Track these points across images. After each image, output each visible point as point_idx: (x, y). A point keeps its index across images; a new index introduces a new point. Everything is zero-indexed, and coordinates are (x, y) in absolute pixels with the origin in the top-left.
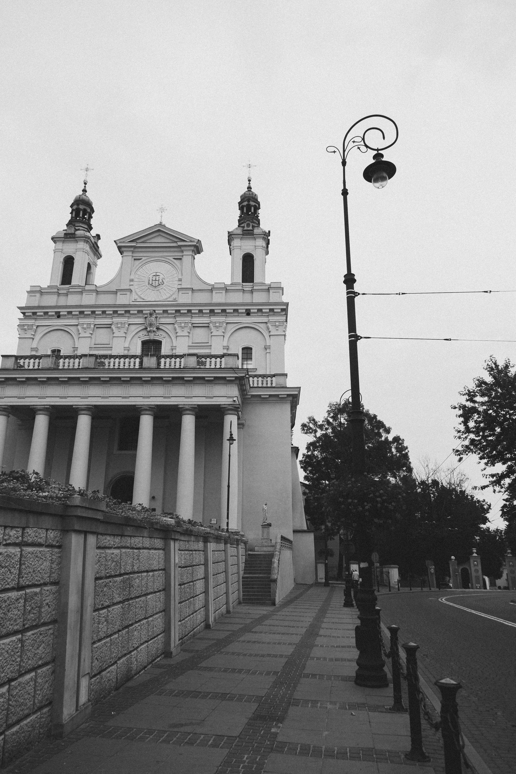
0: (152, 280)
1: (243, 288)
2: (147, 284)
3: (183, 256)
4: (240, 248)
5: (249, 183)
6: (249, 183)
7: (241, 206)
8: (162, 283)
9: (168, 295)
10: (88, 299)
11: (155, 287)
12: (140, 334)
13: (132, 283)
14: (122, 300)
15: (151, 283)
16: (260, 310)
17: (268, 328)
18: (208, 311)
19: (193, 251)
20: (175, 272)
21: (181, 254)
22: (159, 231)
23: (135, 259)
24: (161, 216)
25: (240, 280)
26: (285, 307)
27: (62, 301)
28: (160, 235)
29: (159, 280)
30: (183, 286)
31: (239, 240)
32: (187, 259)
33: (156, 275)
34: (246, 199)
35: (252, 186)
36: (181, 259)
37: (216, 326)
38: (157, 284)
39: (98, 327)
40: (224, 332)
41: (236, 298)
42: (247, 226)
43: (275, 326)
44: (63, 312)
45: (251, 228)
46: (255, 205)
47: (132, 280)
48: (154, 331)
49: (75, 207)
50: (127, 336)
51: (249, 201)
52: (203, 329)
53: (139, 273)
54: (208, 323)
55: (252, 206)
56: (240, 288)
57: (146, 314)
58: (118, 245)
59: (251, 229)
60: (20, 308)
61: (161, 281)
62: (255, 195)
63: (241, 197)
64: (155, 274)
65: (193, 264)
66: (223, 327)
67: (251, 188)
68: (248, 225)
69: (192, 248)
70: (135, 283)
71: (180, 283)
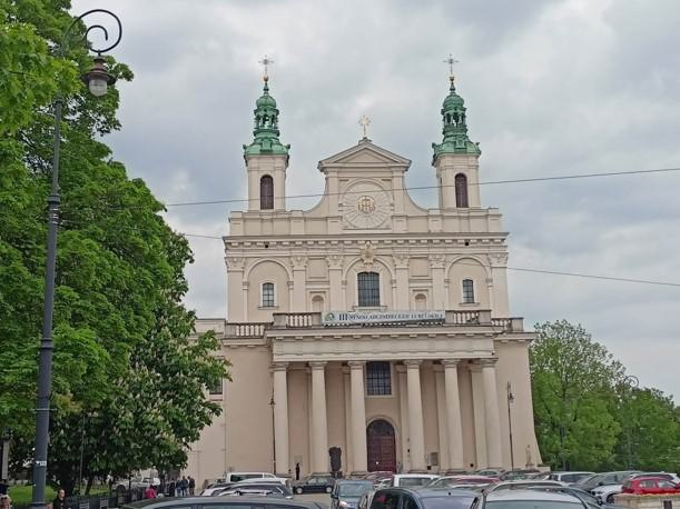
4: (452, 167)
10: (297, 229)
14: (335, 228)
17: (489, 260)
21: (390, 175)
27: (268, 229)
30: (397, 213)
32: (397, 183)
39: (311, 258)
41: (453, 226)
44: (272, 241)
47: (341, 205)
49: (262, 113)
56: (455, 214)
60: (224, 238)
70: (344, 209)
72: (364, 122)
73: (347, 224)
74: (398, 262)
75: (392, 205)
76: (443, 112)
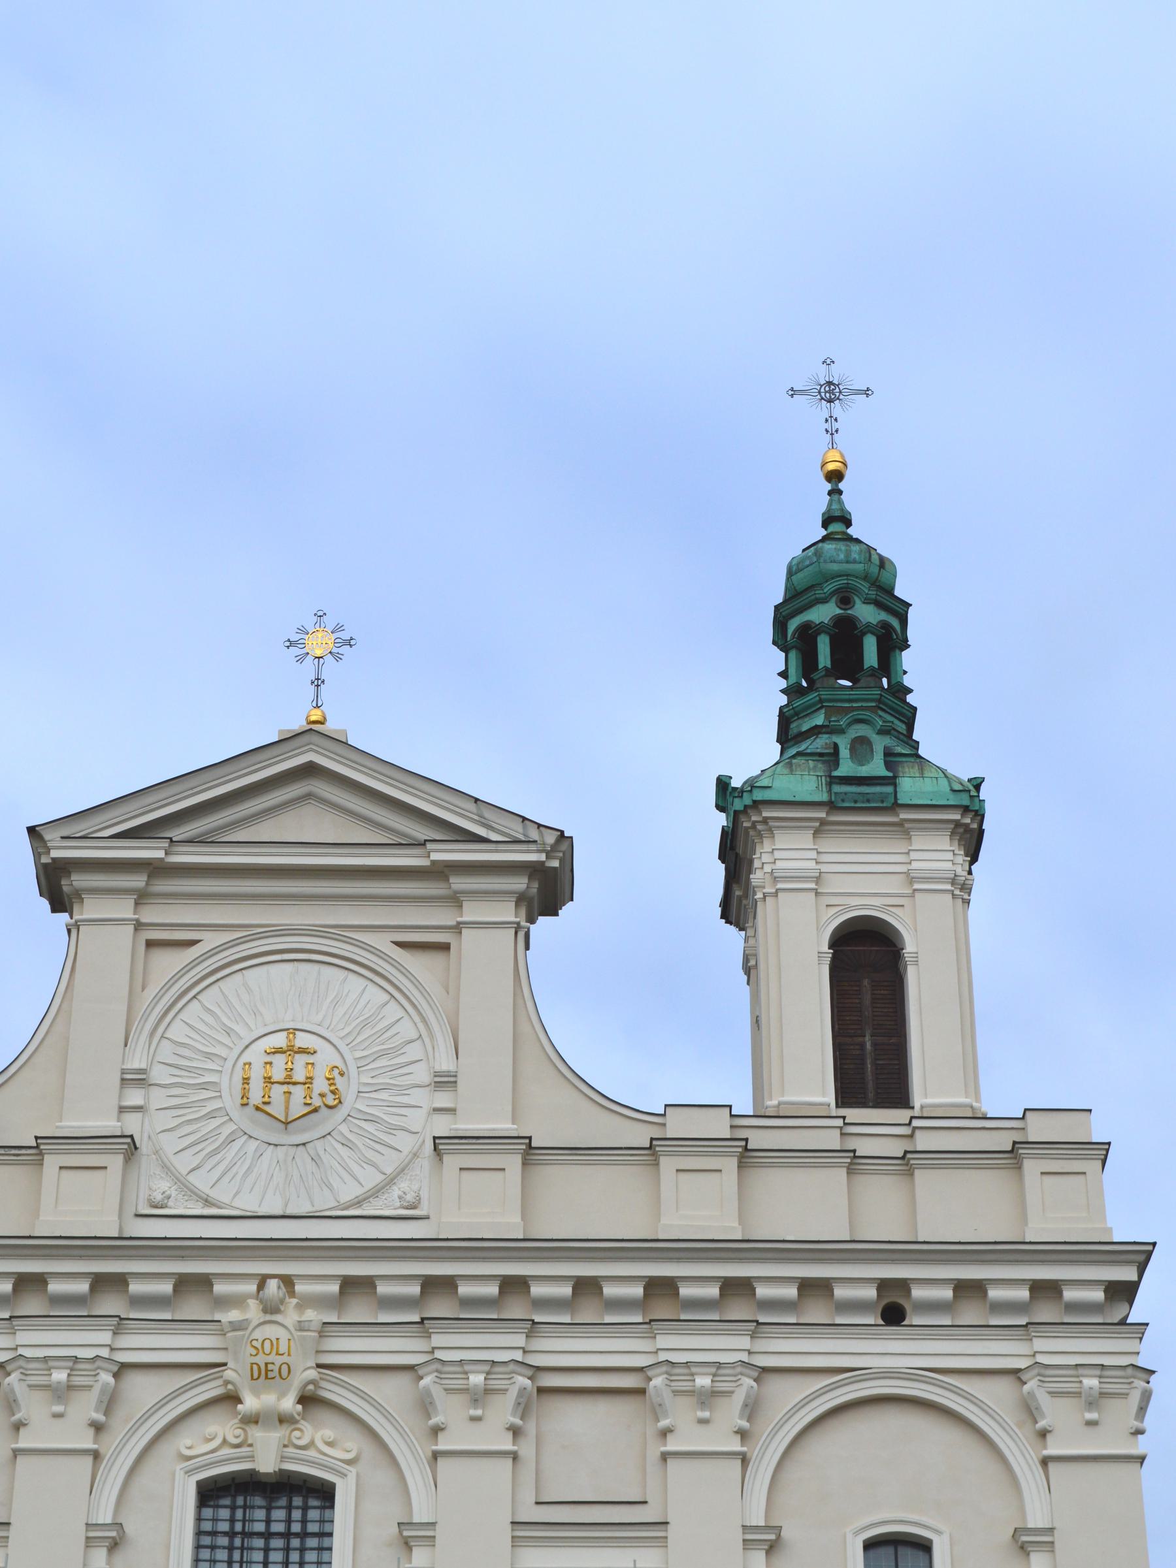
0: (268, 1080)
1: (851, 1144)
2: (230, 1101)
3: (458, 928)
5: (835, 492)
6: (835, 492)
7: (793, 625)
8: (330, 1100)
9: (371, 1179)
11: (287, 1123)
12: (189, 1441)
13: (135, 1097)
15: (256, 1097)
16: (969, 1290)
17: (1030, 1410)
18: (638, 1291)
19: (521, 899)
20: (407, 1029)
21: (445, 917)
22: (310, 770)
23: (150, 944)
24: (318, 682)
25: (831, 1098)
26: (1129, 1274)
28: (309, 796)
29: (309, 1080)
31: (805, 839)
33: (291, 1051)
34: (828, 588)
35: (850, 501)
36: (445, 947)
37: (691, 1393)
38: (297, 1110)
40: (743, 1434)
42: (853, 750)
43: (1078, 1394)
45: (876, 767)
46: (885, 626)
47: (135, 1079)
48: (284, 1420)
50: (108, 1446)
51: (845, 601)
52: (602, 1408)
53: (177, 1031)
54: (641, 1370)
55: (869, 629)
56: (832, 1140)
57: (237, 1301)
58: (54, 854)
59: (883, 772)
61: (320, 1085)
62: (883, 562)
63: (791, 573)
64: (280, 1040)
65: (520, 977)
66: (739, 1398)
67: (848, 523)
68: (861, 747)
69: (520, 883)
70: (158, 1098)
71: (443, 1099)
72: (318, 644)
73: (162, 1186)
74: (450, 1410)
75: (445, 1082)
76: (780, 624)
